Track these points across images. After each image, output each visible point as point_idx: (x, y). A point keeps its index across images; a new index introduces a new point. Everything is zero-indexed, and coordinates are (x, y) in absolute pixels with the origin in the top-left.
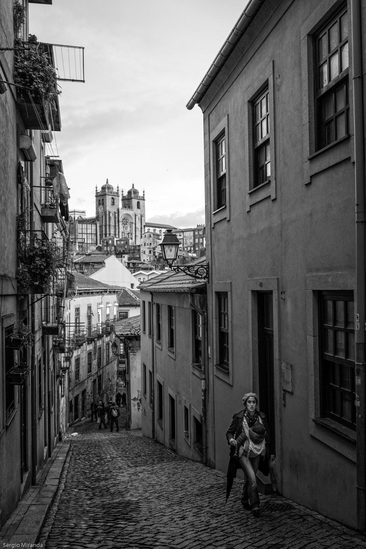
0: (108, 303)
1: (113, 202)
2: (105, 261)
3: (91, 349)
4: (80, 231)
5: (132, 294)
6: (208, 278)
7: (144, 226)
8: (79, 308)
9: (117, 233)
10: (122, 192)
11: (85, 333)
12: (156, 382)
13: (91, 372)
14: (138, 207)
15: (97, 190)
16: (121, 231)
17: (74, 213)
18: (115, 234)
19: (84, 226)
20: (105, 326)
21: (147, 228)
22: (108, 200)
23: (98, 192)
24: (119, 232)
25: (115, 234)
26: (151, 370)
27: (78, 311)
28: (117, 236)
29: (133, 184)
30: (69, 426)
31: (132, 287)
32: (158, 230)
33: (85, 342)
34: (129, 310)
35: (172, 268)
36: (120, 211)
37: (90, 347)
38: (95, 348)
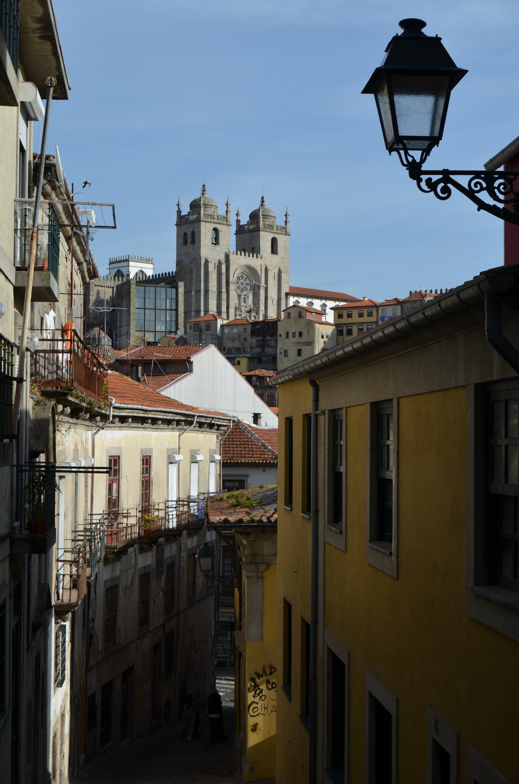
3: (149, 566)
7: (287, 295)
8: (119, 457)
9: (224, 309)
10: (237, 215)
12: (322, 654)
14: (274, 250)
15: (179, 212)
18: (219, 312)
23: (182, 214)
24: (228, 307)
25: (219, 312)
28: (224, 315)
29: (263, 198)
32: (317, 304)
34: (248, 476)
35: (424, 177)
36: (232, 258)
38: (159, 560)
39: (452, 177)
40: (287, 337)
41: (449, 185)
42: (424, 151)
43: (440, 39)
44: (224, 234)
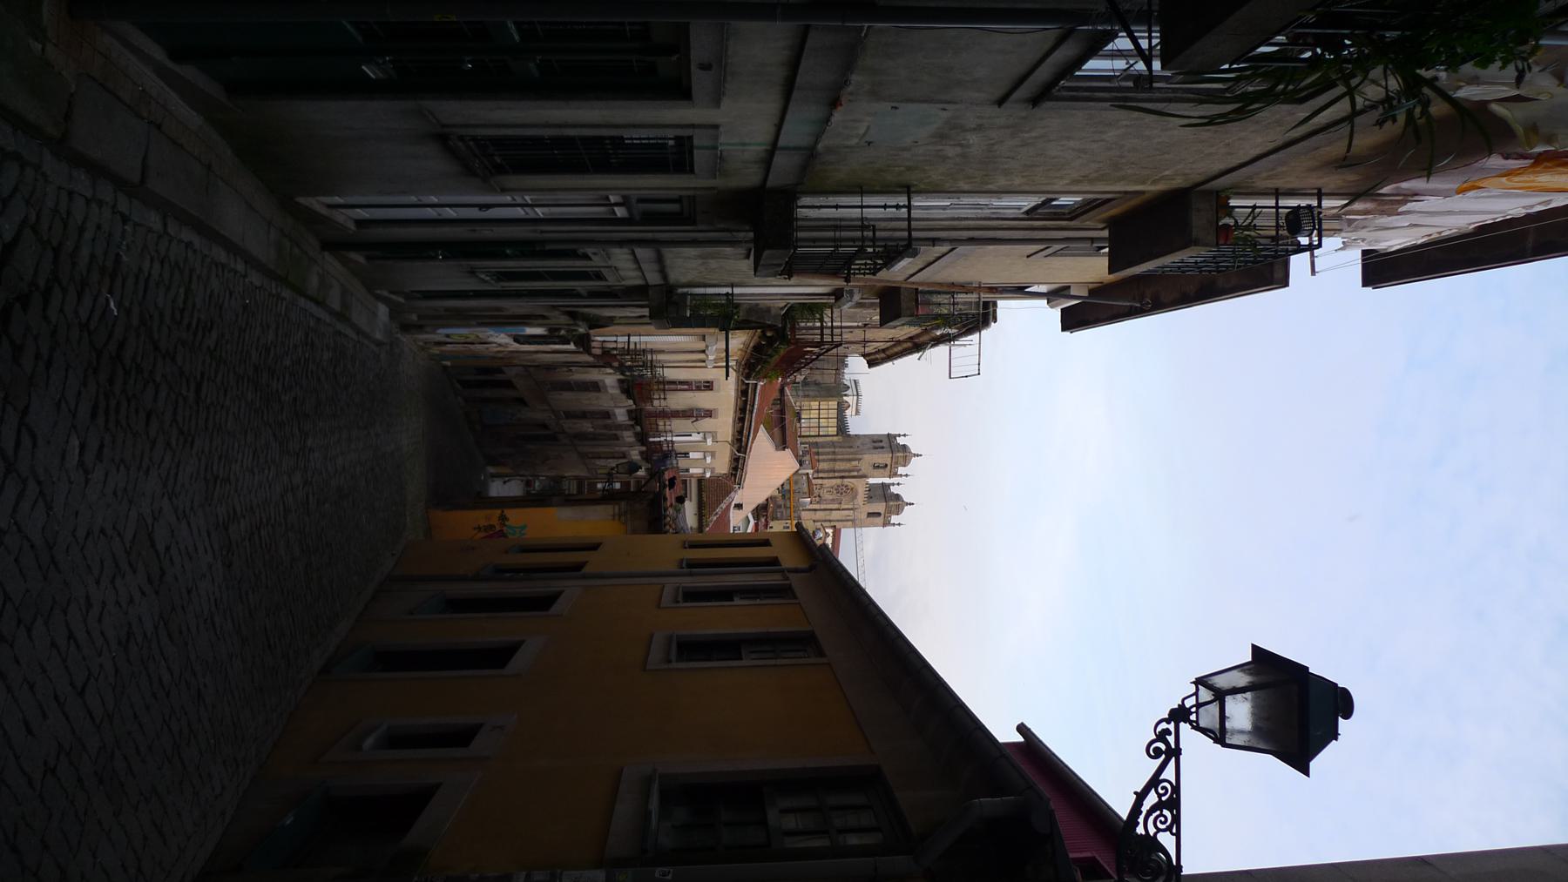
0: (713, 455)
2: (788, 451)
3: (616, 418)
4: (824, 405)
5: (723, 506)
7: (835, 527)
8: (712, 390)
9: (821, 475)
11: (656, 403)
13: (567, 417)
14: (870, 515)
15: (899, 435)
17: (855, 393)
18: (818, 472)
19: (834, 413)
20: (665, 448)
21: (830, 531)
23: (898, 438)
24: (822, 478)
26: (586, 570)
27: (705, 387)
30: (445, 367)
33: (635, 403)
34: (691, 501)
35: (1171, 727)
37: (621, 416)
38: (620, 427)
39: (1173, 761)
41: (1163, 756)
43: (1336, 739)
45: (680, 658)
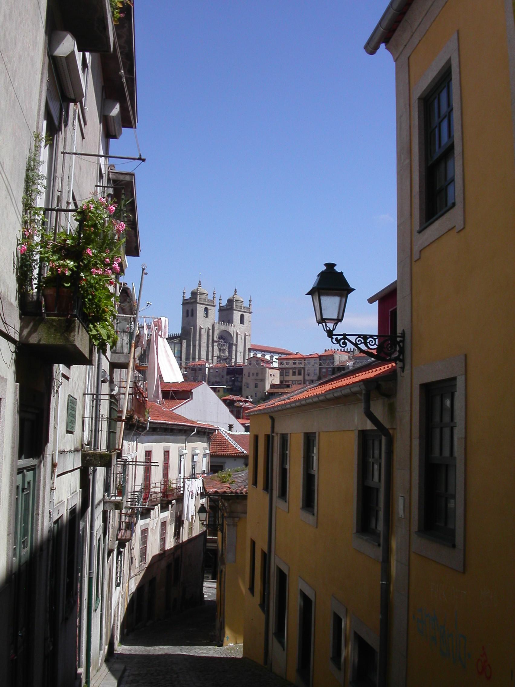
1: (207, 314)
3: (167, 517)
6: (403, 361)
8: (151, 451)
9: (210, 357)
12: (273, 569)
14: (242, 322)
16: (215, 354)
18: (207, 359)
22: (200, 309)
23: (186, 298)
25: (207, 359)
26: (266, 550)
28: (210, 361)
29: (236, 290)
31: (230, 430)
33: (157, 505)
34: (225, 463)
35: (334, 337)
36: (216, 326)
39: (347, 337)
40: (249, 376)
41: (346, 341)
42: (335, 324)
44: (212, 311)
45: (313, 507)
